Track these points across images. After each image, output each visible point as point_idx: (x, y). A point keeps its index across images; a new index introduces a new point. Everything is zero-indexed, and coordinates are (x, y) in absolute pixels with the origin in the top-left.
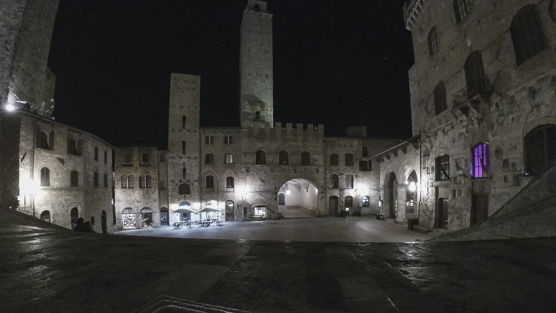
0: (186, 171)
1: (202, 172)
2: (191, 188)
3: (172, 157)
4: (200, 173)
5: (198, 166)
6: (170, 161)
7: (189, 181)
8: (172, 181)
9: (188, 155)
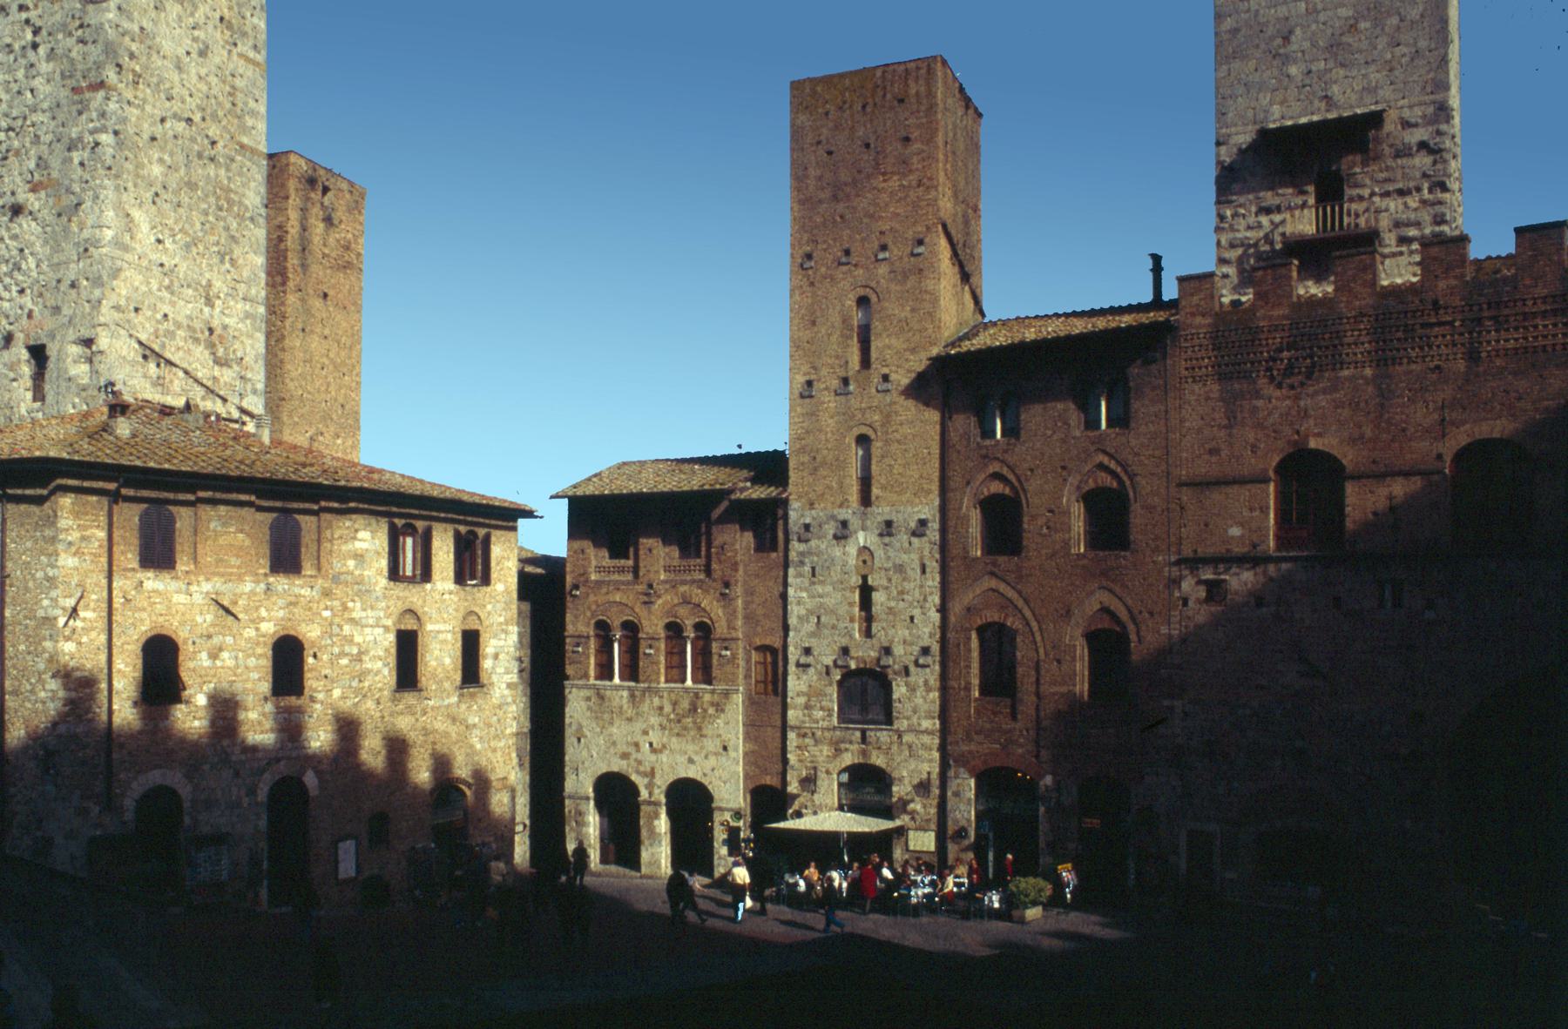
0: (878, 597)
1: (956, 608)
2: (899, 690)
3: (807, 527)
4: (943, 609)
5: (933, 566)
6: (796, 547)
7: (887, 651)
8: (808, 651)
9: (881, 511)
